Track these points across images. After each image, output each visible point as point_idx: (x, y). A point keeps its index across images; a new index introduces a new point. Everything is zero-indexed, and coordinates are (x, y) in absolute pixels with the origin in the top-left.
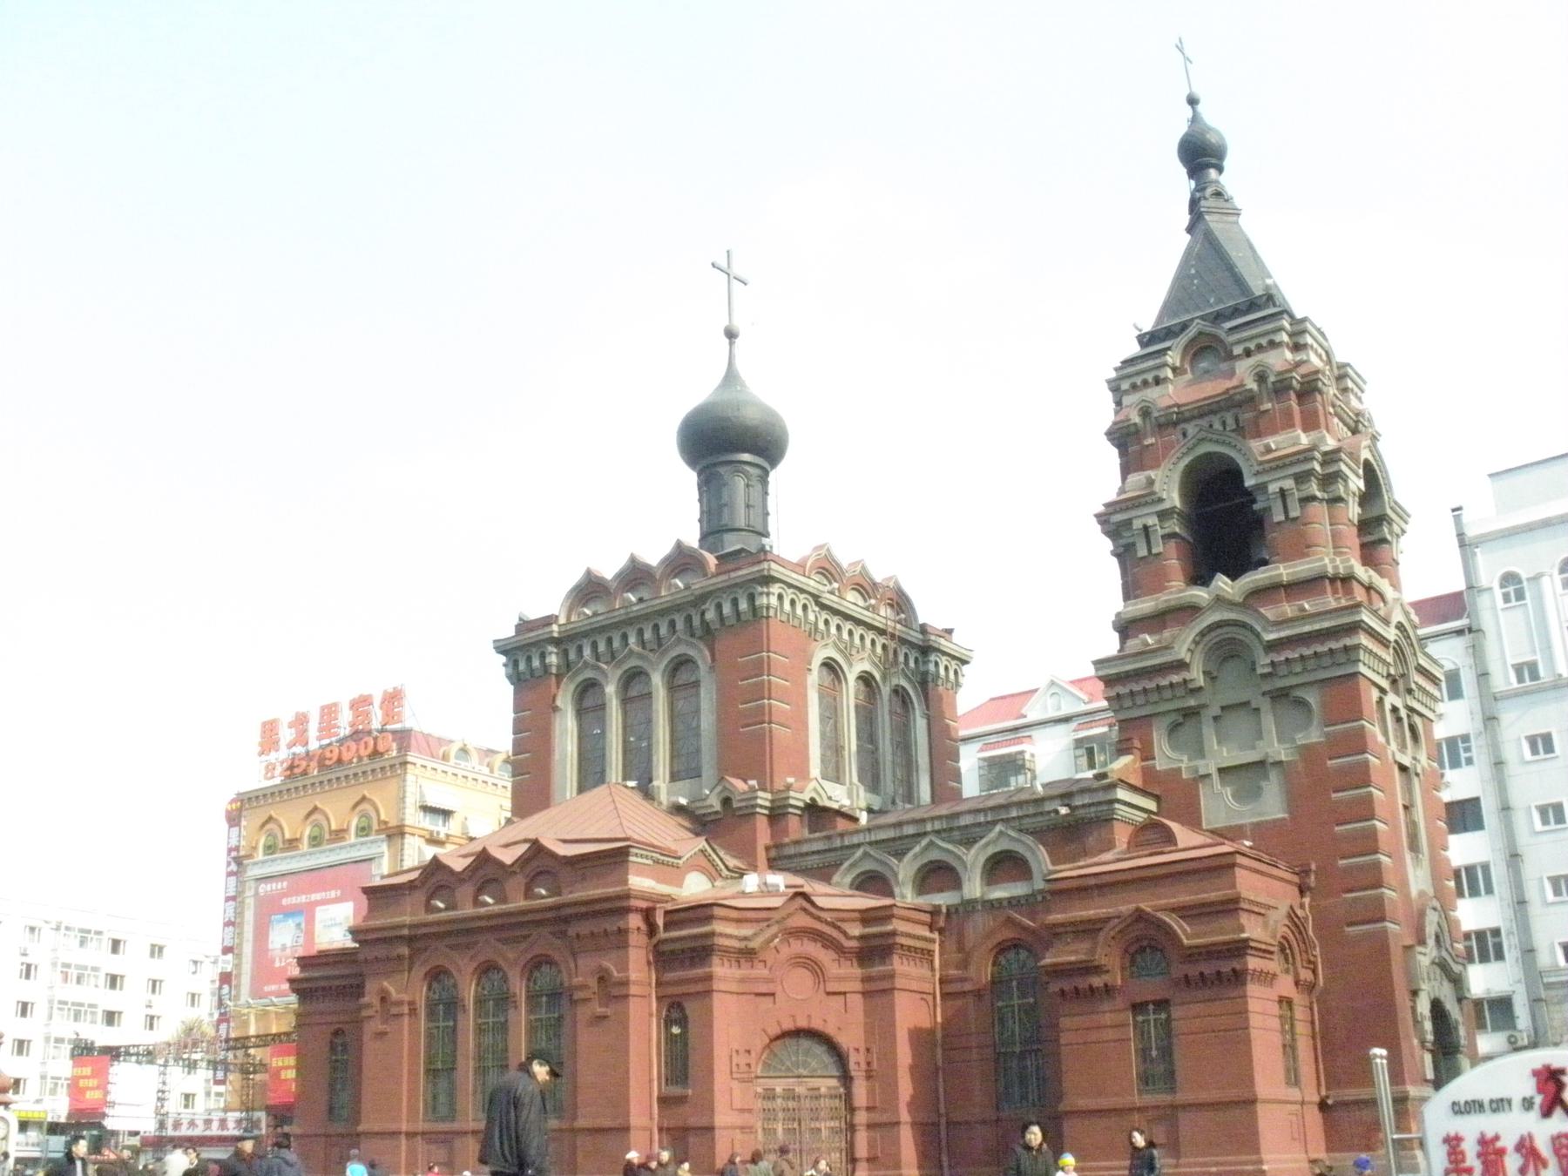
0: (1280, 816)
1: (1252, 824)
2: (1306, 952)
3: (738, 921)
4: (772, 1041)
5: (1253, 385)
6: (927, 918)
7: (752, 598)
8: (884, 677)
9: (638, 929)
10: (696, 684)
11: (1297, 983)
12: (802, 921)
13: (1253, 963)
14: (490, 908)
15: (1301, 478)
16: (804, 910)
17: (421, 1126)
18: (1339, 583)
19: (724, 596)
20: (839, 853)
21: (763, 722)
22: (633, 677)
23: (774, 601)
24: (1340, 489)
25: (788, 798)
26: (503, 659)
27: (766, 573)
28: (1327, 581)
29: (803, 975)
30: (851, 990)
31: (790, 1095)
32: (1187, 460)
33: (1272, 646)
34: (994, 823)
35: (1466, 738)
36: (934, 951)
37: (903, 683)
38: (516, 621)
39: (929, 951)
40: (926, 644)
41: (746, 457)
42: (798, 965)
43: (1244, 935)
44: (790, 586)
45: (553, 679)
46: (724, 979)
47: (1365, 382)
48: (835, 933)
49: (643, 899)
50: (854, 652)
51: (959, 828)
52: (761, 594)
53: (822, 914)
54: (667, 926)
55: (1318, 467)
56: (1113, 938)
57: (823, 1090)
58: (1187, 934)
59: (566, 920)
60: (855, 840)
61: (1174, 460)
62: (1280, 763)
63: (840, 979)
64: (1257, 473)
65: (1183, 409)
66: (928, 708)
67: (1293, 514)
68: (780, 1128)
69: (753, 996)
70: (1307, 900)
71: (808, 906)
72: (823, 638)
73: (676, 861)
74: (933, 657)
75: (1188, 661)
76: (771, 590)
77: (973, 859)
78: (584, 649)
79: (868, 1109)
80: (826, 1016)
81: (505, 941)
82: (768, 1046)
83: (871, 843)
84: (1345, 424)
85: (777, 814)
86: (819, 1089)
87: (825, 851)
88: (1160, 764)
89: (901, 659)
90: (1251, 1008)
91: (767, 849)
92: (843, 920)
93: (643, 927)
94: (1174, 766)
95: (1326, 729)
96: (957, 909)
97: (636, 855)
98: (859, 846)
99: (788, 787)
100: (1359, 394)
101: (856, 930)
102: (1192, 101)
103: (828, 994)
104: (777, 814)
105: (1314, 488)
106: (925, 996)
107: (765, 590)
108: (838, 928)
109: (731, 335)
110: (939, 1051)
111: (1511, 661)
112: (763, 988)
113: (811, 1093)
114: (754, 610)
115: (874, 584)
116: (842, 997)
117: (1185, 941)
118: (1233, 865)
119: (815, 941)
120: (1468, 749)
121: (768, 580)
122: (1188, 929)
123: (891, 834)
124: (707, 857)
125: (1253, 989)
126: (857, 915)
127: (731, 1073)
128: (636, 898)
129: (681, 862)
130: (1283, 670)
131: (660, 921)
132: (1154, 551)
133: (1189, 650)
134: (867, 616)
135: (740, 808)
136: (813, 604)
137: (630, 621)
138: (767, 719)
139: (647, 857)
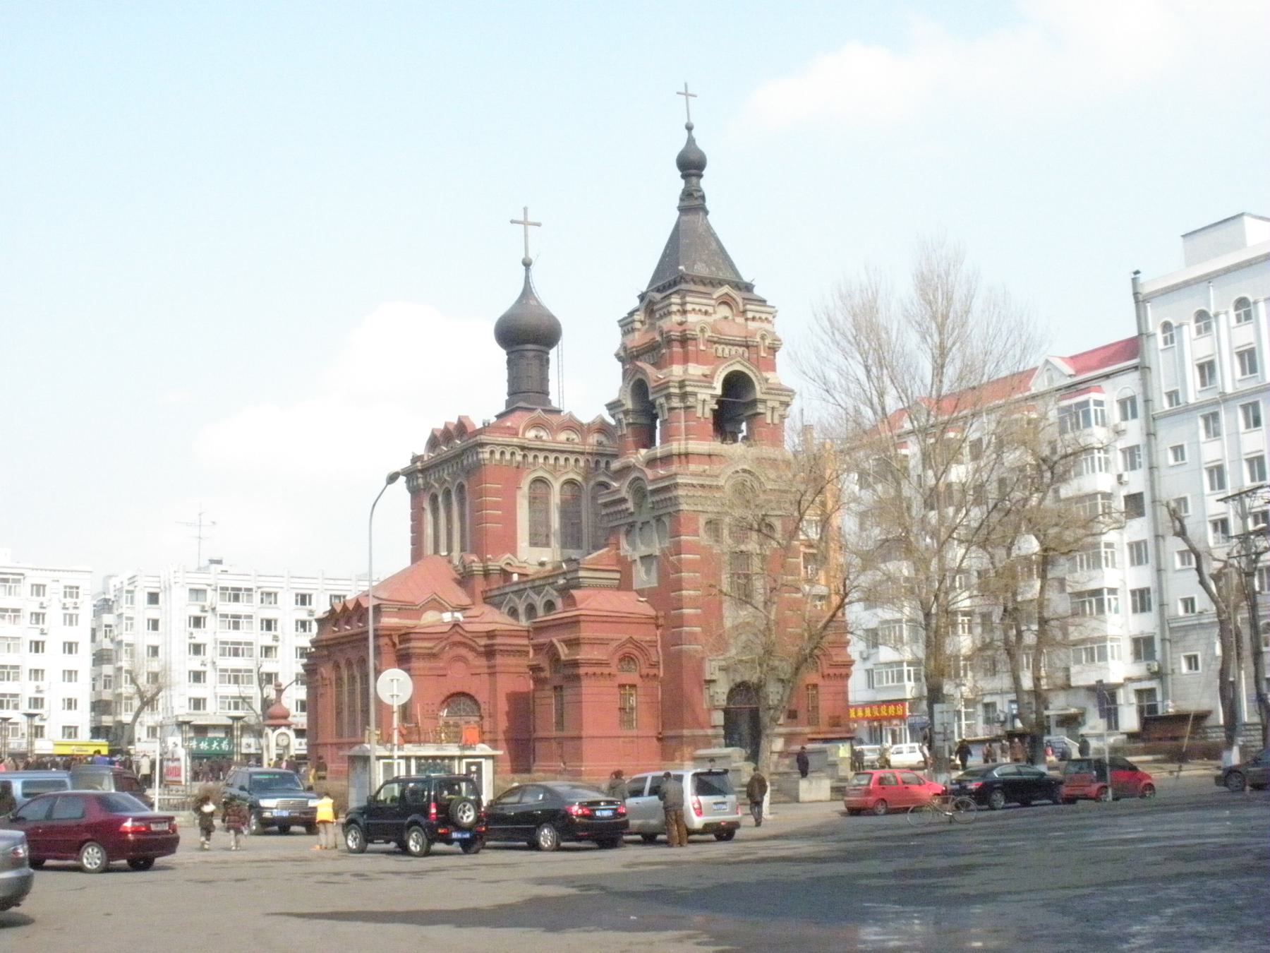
0: (656, 585)
4: (449, 697)
5: (658, 338)
6: (526, 634)
8: (586, 479)
11: (641, 676)
12: (458, 638)
15: (668, 397)
17: (335, 740)
18: (683, 457)
22: (447, 493)
23: (487, 456)
29: (460, 666)
32: (631, 383)
34: (544, 585)
35: (1138, 446)
38: (410, 457)
41: (529, 346)
44: (499, 445)
47: (773, 307)
54: (400, 643)
55: (676, 391)
58: (564, 652)
60: (507, 590)
63: (479, 667)
67: (666, 417)
77: (539, 602)
80: (471, 686)
81: (353, 647)
82: (443, 702)
93: (390, 643)
98: (507, 594)
99: (490, 559)
100: (764, 316)
101: (483, 642)
102: (689, 128)
104: (486, 574)
105: (675, 403)
109: (527, 264)
111: (1165, 389)
114: (479, 460)
115: (582, 425)
117: (563, 658)
118: (578, 622)
120: (1140, 457)
121: (482, 445)
122: (566, 651)
124: (438, 602)
125: (585, 682)
130: (656, 507)
131: (397, 641)
134: (569, 447)
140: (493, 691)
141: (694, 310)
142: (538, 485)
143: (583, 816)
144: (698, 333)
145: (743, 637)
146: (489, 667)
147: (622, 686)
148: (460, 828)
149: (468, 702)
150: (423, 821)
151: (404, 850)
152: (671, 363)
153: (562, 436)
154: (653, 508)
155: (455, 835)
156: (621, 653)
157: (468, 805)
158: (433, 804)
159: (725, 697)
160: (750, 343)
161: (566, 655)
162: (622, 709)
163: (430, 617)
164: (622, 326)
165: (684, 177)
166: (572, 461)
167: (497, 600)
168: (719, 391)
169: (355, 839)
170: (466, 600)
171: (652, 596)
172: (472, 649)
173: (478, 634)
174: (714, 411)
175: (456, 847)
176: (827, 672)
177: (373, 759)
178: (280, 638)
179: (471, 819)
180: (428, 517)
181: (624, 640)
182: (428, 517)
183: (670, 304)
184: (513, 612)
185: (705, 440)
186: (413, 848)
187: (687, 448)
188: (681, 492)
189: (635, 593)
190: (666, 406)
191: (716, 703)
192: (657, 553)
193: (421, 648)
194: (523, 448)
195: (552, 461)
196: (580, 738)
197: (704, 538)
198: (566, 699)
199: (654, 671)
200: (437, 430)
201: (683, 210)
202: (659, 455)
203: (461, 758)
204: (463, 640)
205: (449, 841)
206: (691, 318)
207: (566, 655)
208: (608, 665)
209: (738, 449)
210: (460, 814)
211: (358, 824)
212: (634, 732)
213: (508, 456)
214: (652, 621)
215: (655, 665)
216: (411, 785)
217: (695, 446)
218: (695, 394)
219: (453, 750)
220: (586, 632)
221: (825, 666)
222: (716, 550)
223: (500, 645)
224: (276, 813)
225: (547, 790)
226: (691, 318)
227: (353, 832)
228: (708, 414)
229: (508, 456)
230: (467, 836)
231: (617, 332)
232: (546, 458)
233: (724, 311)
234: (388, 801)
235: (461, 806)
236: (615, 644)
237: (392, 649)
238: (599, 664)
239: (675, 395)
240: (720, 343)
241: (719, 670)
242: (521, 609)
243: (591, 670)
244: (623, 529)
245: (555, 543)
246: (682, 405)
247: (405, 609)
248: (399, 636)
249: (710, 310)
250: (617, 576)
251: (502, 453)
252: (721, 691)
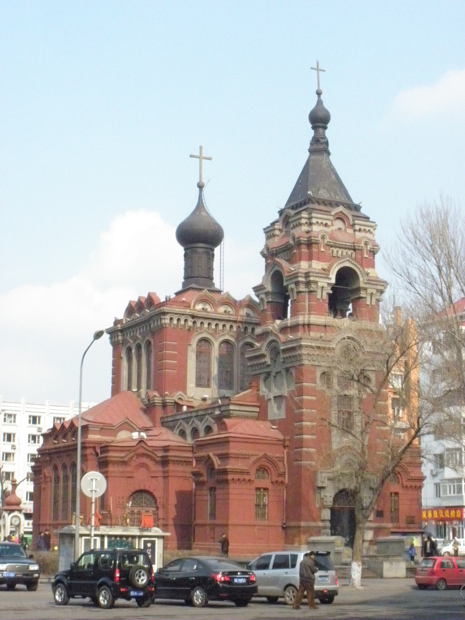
1: (279, 420)
2: (277, 470)
3: (122, 451)
4: (134, 493)
5: (291, 242)
6: (191, 449)
7: (161, 319)
8: (237, 339)
9: (91, 454)
11: (272, 482)
12: (142, 451)
13: (230, 477)
14: (66, 444)
15: (297, 283)
16: (142, 447)
17: (52, 522)
18: (306, 327)
21: (163, 369)
22: (139, 347)
23: (168, 321)
24: (313, 287)
25: (165, 400)
27: (162, 311)
28: (301, 327)
29: (143, 470)
32: (272, 272)
33: (284, 351)
34: (205, 415)
38: (114, 321)
41: (201, 245)
43: (227, 467)
44: (176, 314)
45: (121, 345)
46: (114, 472)
47: (375, 222)
52: (163, 319)
53: (149, 449)
54: (101, 452)
56: (204, 464)
60: (178, 417)
61: (269, 272)
62: (285, 396)
63: (156, 472)
64: (287, 281)
65: (277, 249)
67: (295, 298)
70: (285, 451)
71: (143, 445)
75: (265, 354)
76: (166, 317)
77: (201, 427)
79: (163, 519)
80: (150, 485)
82: (131, 495)
83: (182, 419)
84: (345, 248)
85: (164, 405)
88: (261, 394)
90: (230, 492)
91: (161, 419)
93: (94, 453)
94: (264, 394)
95: (296, 385)
97: (92, 427)
98: (179, 420)
99: (167, 395)
100: (367, 229)
101: (160, 454)
103: (152, 477)
104: (164, 405)
105: (302, 288)
106: (188, 478)
108: (153, 453)
109: (201, 187)
112: (129, 475)
114: (162, 324)
115: (236, 301)
116: (156, 479)
117: (216, 467)
118: (228, 442)
119: (148, 458)
121: (164, 313)
122: (219, 462)
124: (129, 425)
125: (232, 485)
126: (162, 448)
128: (89, 443)
129: (115, 428)
131: (99, 451)
132: (265, 308)
133: (266, 350)
134: (226, 317)
136: (190, 318)
138: (164, 368)
139: (96, 428)
140: (166, 490)
141: (317, 222)
142: (203, 343)
143: (224, 582)
144: (320, 239)
145: (345, 458)
146: (164, 472)
147: (258, 489)
148: (136, 588)
149: (149, 497)
150: (110, 583)
151: (96, 603)
152: (300, 260)
153: (222, 309)
154: (284, 362)
155: (132, 593)
156: (258, 464)
157: (143, 572)
158: (117, 570)
159: (332, 500)
160: (357, 247)
161: (219, 466)
162: (257, 505)
163: (123, 435)
164: (266, 233)
165: (314, 128)
166: (228, 327)
167: (171, 424)
168: (333, 281)
169: (61, 595)
170: (149, 424)
171: (282, 425)
172: (152, 459)
173: (156, 448)
174: (329, 294)
175: (133, 602)
176: (405, 484)
177: (77, 536)
178: (17, 447)
179: (144, 581)
180: (125, 364)
181: (260, 455)
182: (125, 364)
183: (301, 218)
184: (183, 434)
185: (322, 315)
186: (102, 602)
187: (309, 320)
188: (304, 351)
189: (268, 424)
190: (295, 290)
191: (325, 504)
192: (286, 394)
193: (117, 457)
194: (193, 317)
195: (213, 327)
196: (226, 525)
197: (319, 385)
198: (218, 497)
199: (280, 479)
200: (133, 302)
201: (311, 151)
202: (289, 325)
203: (140, 537)
205: (129, 598)
206: (315, 228)
207: (219, 466)
208: (248, 473)
209: (345, 322)
210: (137, 578)
211: (63, 583)
212: (266, 523)
213: (182, 322)
214: (281, 443)
215: (282, 475)
216: (103, 556)
217: (315, 319)
218: (316, 282)
219: (135, 531)
220: (233, 449)
221: (404, 480)
222: (328, 393)
223: (171, 456)
224: (5, 574)
225: (199, 562)
226: (315, 228)
227: (60, 589)
228: (325, 296)
229: (182, 322)
230: (141, 594)
231: (263, 236)
232: (209, 324)
233: (339, 224)
234: (86, 567)
235: (137, 572)
236: (253, 459)
237: (95, 457)
238: (242, 472)
239: (302, 282)
240: (336, 247)
241: (328, 479)
242: (188, 431)
243: (236, 477)
244: (262, 377)
245: (214, 385)
246: (307, 290)
247: (105, 428)
248: (101, 448)
249: (329, 223)
250: (257, 410)
251: (179, 320)
252: (329, 495)
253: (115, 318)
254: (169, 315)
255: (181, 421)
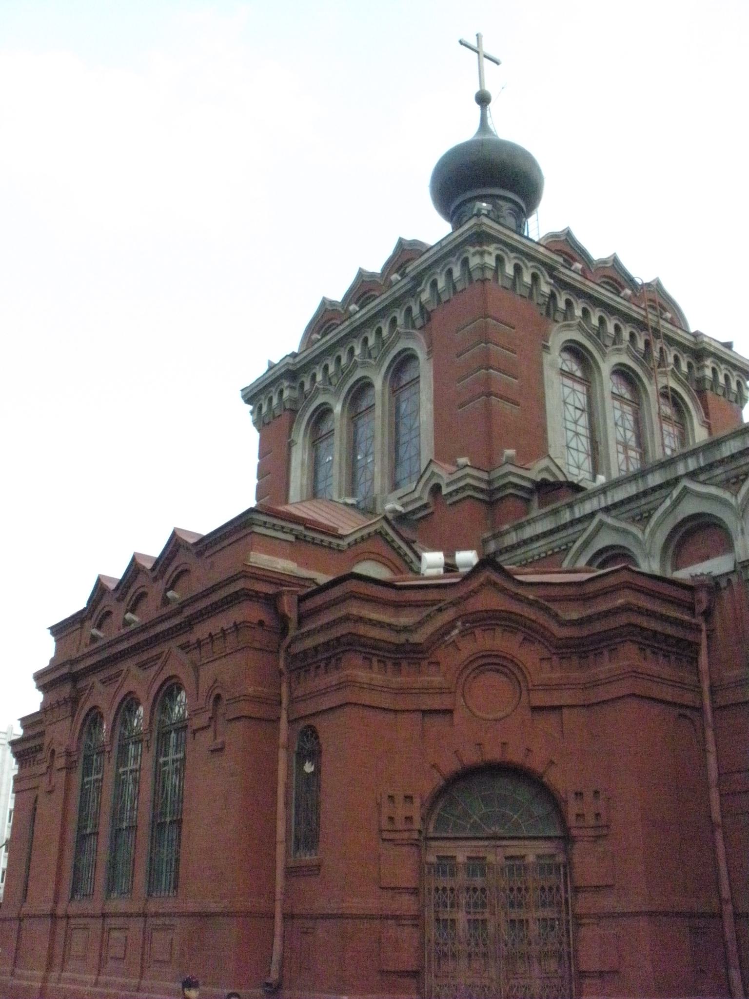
3: (398, 606)
9: (261, 623)
10: (416, 380)
16: (495, 584)
19: (438, 271)
20: (570, 531)
23: (491, 261)
26: (250, 407)
30: (569, 702)
31: (477, 864)
36: (698, 644)
37: (673, 384)
39: (690, 644)
40: (698, 347)
42: (481, 669)
48: (542, 619)
49: (271, 582)
50: (608, 342)
51: (722, 462)
57: (531, 858)
59: (188, 625)
60: (588, 507)
63: (548, 687)
66: (707, 414)
68: (461, 917)
69: (418, 716)
71: (495, 577)
72: (565, 319)
73: (335, 541)
74: (709, 362)
76: (485, 248)
78: (317, 376)
83: (607, 510)
86: (523, 857)
87: (551, 532)
89: (671, 359)
92: (554, 600)
96: (729, 581)
98: (592, 515)
103: (536, 709)
106: (688, 712)
107: (477, 248)
108: (546, 610)
110: (714, 795)
112: (435, 703)
113: (508, 863)
123: (631, 490)
127: (381, 831)
129: (344, 543)
135: (450, 494)
136: (546, 274)
137: (355, 332)
166: (626, 334)
204: (516, 608)
229: (527, 279)
253: (270, 362)
254: (494, 246)
255: (600, 516)
